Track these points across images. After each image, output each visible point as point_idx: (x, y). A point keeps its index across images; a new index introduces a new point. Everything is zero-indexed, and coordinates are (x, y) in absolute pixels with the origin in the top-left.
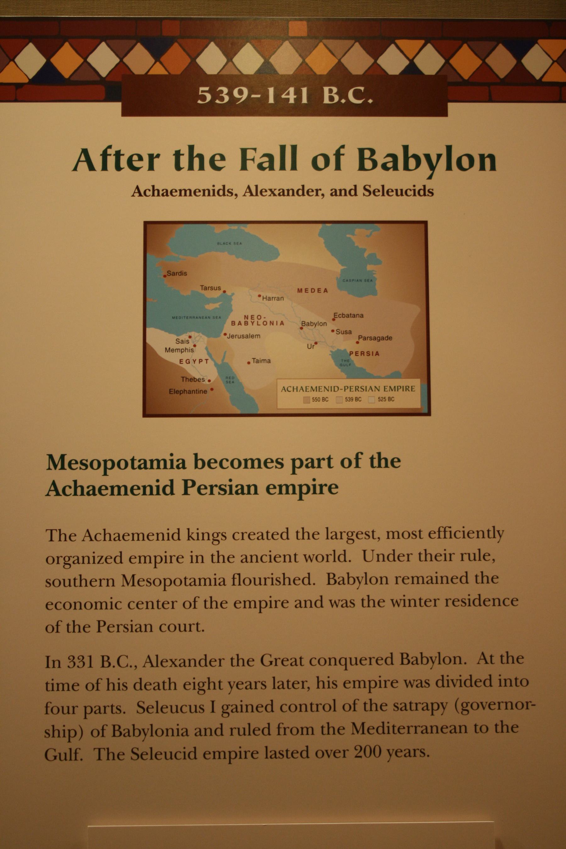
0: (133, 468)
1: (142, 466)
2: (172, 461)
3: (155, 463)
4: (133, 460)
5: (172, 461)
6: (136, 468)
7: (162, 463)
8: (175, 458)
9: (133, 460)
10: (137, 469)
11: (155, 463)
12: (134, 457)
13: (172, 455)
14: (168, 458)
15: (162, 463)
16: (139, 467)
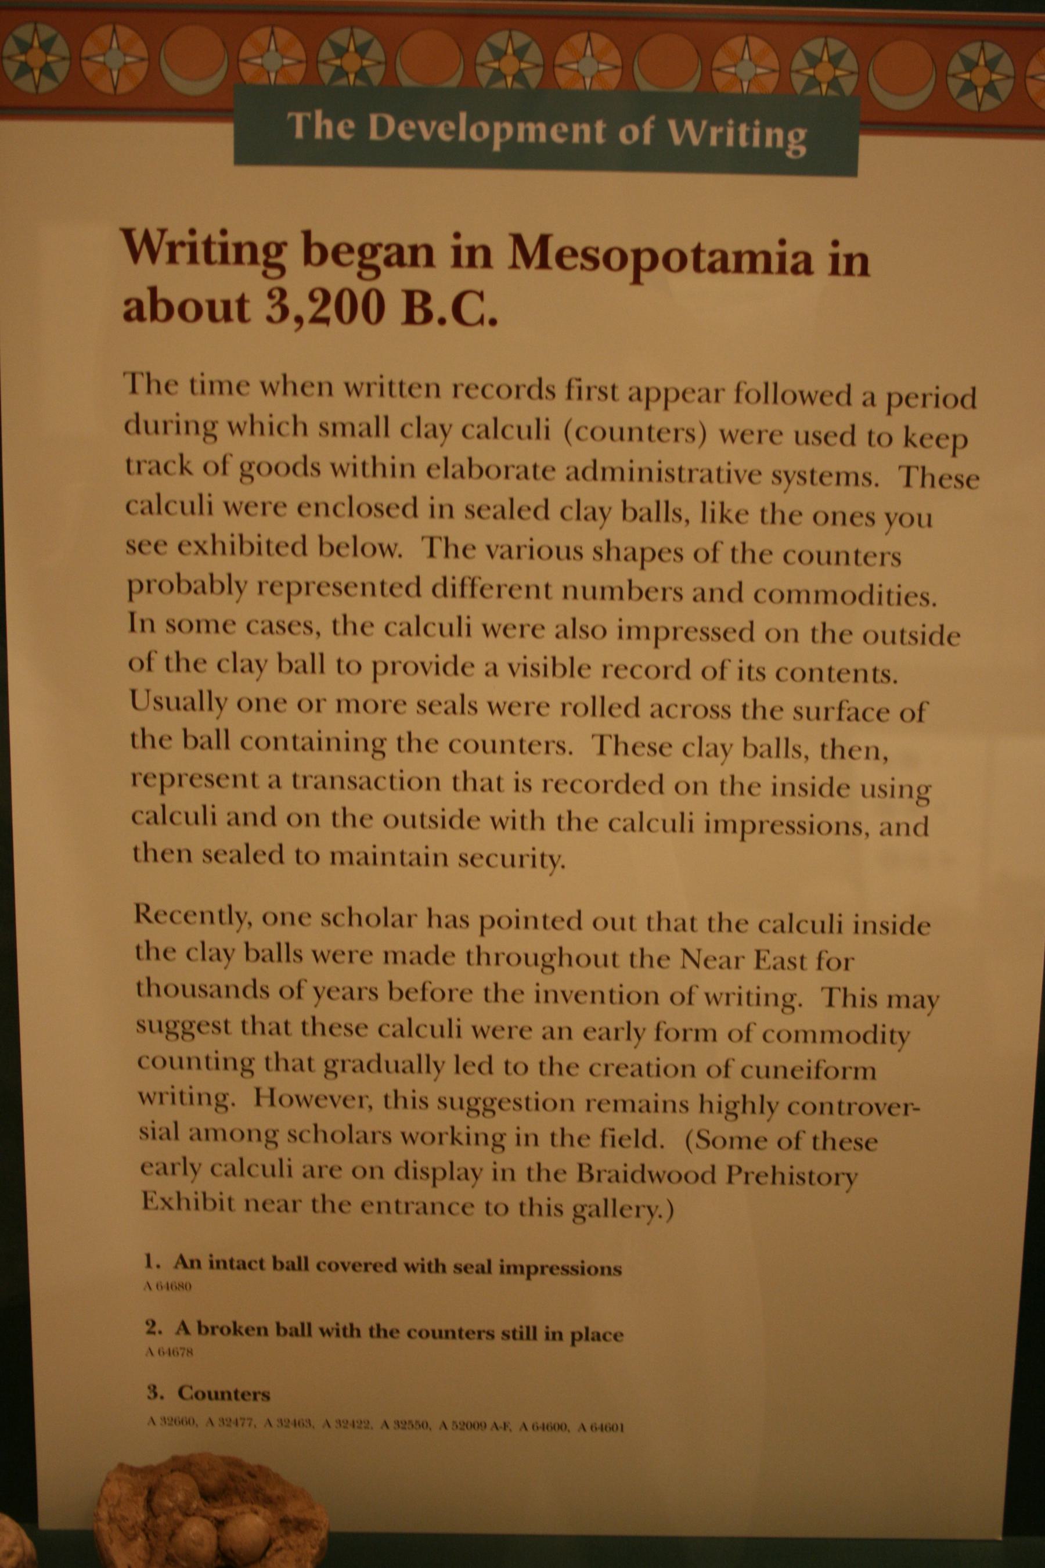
0: (697, 268)
1: (718, 266)
2: (782, 256)
3: (746, 260)
4: (697, 251)
5: (782, 256)
6: (704, 270)
7: (761, 261)
8: (789, 250)
9: (697, 251)
10: (707, 272)
11: (746, 260)
12: (699, 245)
13: (782, 242)
14: (774, 249)
15: (761, 261)
16: (711, 268)
